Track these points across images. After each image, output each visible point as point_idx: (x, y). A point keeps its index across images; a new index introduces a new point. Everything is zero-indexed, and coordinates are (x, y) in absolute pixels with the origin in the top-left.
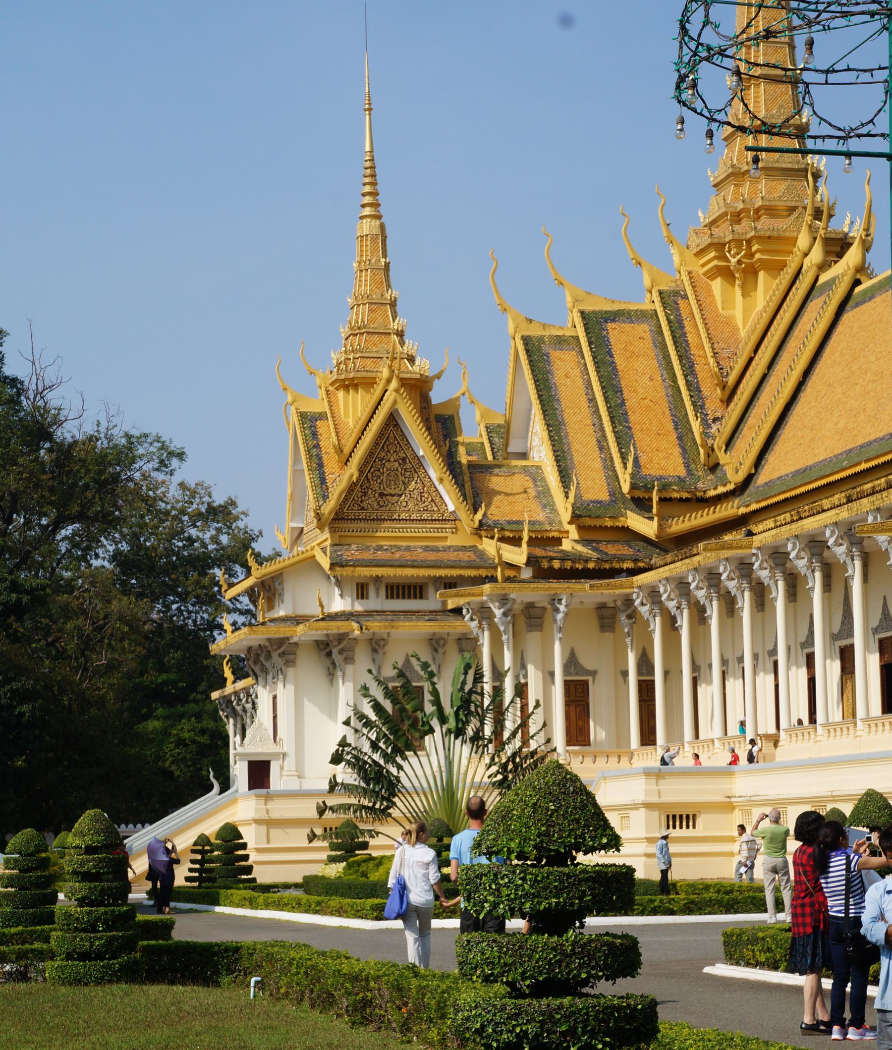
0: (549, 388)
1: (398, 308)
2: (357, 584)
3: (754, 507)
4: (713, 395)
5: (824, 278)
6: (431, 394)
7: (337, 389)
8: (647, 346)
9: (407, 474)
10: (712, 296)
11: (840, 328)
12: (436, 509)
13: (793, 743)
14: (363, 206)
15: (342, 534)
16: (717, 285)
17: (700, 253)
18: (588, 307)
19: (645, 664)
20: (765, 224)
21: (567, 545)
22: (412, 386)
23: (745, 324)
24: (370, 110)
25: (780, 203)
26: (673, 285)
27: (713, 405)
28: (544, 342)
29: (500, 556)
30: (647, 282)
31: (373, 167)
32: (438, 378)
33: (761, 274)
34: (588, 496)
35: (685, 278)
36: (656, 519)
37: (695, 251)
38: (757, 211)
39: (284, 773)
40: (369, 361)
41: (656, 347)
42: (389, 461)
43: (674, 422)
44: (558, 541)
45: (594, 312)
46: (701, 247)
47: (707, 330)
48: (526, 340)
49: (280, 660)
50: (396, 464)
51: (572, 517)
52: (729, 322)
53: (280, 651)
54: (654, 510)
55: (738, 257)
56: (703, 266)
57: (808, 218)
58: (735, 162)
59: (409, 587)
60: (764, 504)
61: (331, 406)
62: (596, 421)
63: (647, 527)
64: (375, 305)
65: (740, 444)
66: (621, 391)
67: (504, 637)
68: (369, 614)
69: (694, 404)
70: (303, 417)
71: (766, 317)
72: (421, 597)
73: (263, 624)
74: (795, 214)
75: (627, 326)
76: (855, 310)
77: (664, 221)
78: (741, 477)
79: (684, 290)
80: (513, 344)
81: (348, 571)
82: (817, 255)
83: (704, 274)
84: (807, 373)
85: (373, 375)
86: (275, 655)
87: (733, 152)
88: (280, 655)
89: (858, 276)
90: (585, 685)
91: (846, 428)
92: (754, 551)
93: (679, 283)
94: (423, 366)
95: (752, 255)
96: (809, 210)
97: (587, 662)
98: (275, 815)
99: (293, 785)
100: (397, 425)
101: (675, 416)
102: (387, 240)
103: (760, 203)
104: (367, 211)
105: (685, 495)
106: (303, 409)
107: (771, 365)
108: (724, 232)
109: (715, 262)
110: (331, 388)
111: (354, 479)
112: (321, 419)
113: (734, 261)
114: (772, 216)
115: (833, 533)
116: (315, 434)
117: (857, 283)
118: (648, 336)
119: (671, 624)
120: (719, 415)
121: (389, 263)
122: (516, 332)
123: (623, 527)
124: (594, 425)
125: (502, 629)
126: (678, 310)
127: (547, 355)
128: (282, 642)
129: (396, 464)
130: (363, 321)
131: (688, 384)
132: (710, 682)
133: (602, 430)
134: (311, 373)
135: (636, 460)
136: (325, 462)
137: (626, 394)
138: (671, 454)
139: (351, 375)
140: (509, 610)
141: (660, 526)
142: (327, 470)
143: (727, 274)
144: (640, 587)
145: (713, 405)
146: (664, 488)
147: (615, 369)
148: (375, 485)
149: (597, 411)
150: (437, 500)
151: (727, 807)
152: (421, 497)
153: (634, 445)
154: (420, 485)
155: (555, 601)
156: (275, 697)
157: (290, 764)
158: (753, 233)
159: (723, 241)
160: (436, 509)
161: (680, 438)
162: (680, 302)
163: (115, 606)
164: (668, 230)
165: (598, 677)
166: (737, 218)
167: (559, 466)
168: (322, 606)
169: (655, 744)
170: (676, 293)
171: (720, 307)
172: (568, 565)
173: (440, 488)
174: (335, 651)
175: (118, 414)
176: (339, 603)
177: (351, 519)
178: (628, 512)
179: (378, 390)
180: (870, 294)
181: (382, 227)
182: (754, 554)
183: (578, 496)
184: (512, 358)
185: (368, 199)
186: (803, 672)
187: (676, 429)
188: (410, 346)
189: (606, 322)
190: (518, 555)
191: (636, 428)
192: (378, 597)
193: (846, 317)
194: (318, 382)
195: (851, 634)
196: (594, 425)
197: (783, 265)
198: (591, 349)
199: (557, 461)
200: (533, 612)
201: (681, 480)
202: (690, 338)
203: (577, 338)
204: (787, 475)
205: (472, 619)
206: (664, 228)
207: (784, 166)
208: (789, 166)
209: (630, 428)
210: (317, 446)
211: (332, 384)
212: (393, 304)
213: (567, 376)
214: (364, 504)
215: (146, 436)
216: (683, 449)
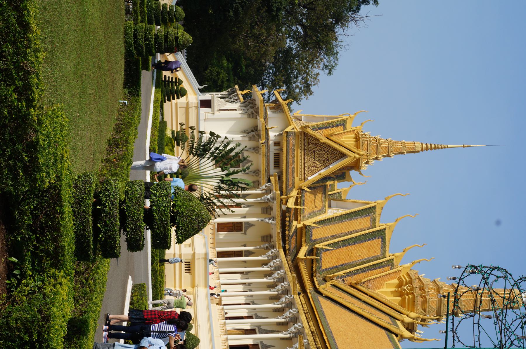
0: (356, 216)
1: (387, 158)
2: (280, 142)
3: (310, 296)
4: (353, 280)
5: (399, 323)
6: (353, 171)
7: (355, 134)
8: (372, 254)
9: (322, 161)
10: (392, 279)
11: (379, 329)
13: (222, 342)
14: (426, 144)
15: (299, 136)
16: (396, 281)
17: (408, 275)
18: (387, 231)
19: (249, 253)
20: (420, 300)
21: (295, 223)
22: (357, 163)
23: (381, 292)
24: (464, 147)
25: (427, 306)
27: (349, 280)
28: (373, 214)
29: (290, 197)
30: (397, 254)
31: (441, 148)
32: (360, 173)
33: (400, 298)
34: (314, 231)
35: (399, 269)
36: (305, 258)
37: (409, 273)
38: (425, 297)
39: (206, 114)
40: (366, 146)
41: (372, 258)
43: (343, 265)
44: (296, 220)
45: (385, 234)
46: (410, 275)
47: (378, 278)
48: (374, 207)
49: (250, 112)
50: (326, 157)
52: (381, 286)
53: (254, 112)
54: (308, 257)
55: (407, 289)
56: (403, 276)
57: (422, 316)
58: (444, 288)
59: (279, 162)
60: (311, 299)
61: (349, 132)
62: (343, 235)
63: (302, 254)
64: (388, 149)
65: (334, 290)
66: (355, 244)
67: (259, 199)
68: (268, 146)
69: (350, 272)
70: (345, 121)
71: (383, 300)
72: (275, 167)
73: (264, 105)
74: (423, 312)
75: (380, 246)
76: (386, 335)
77: (421, 261)
78: (321, 290)
79: (394, 269)
80: (373, 202)
81: (285, 138)
82: (407, 320)
83: (400, 276)
84: (362, 316)
85: (361, 148)
86: (252, 110)
87: (447, 287)
88: (252, 112)
89: (399, 336)
90: (241, 230)
92: (293, 296)
93: (397, 266)
94: (364, 167)
95: (407, 295)
96: (425, 317)
97: (250, 231)
98: (190, 110)
99: (202, 117)
100: (341, 157)
102: (413, 154)
103: (427, 298)
104: (424, 146)
105: (314, 269)
106: (348, 121)
107: (364, 302)
108: (416, 284)
109: (404, 281)
110: (356, 132)
111: (321, 141)
112: (344, 128)
113: (405, 288)
114: (422, 303)
115: (300, 326)
116: (338, 125)
117: (397, 335)
118: (376, 254)
119: (264, 263)
120: (345, 282)
123: (302, 245)
125: (262, 198)
126: (386, 266)
127: (369, 215)
128: (257, 113)
129: (326, 157)
130: (382, 144)
131: (357, 270)
132: (242, 278)
133: (340, 237)
134: (362, 124)
135: (328, 250)
136: (327, 130)
137: (353, 246)
139: (361, 140)
140: (270, 201)
141: (302, 259)
142: (324, 130)
143: (400, 285)
144: (278, 251)
145: (349, 280)
146: (317, 261)
147: (364, 242)
148: (318, 149)
149: (347, 235)
150: (312, 173)
151: (193, 285)
154: (318, 166)
155: (273, 218)
156: (236, 110)
157: (210, 116)
158: (416, 295)
159: (413, 283)
161: (336, 267)
162: (389, 267)
163: (271, 48)
164: (417, 262)
165: (244, 235)
166: (422, 289)
167: (325, 220)
168: (271, 128)
169: (218, 257)
170: (393, 265)
172: (287, 224)
173: (317, 174)
174: (254, 133)
175: (346, 49)
176: (272, 135)
178: (307, 247)
180: (392, 341)
181: (418, 152)
182: (291, 296)
183: (314, 227)
184: (367, 202)
185: (429, 146)
186: (246, 315)
187: (340, 265)
188: (372, 162)
189: (382, 238)
190: (291, 204)
192: (276, 150)
193: (383, 332)
194: (358, 127)
195: (260, 333)
197: (403, 307)
198: (371, 232)
199: (327, 219)
200: (269, 210)
201: (320, 267)
202: (375, 271)
203: (375, 227)
204: (322, 308)
205: (266, 186)
206: (418, 261)
207: (442, 307)
208: (442, 309)
209: (340, 247)
210: (333, 126)
211: (357, 132)
212: (388, 156)
214: (311, 145)
215: (337, 60)
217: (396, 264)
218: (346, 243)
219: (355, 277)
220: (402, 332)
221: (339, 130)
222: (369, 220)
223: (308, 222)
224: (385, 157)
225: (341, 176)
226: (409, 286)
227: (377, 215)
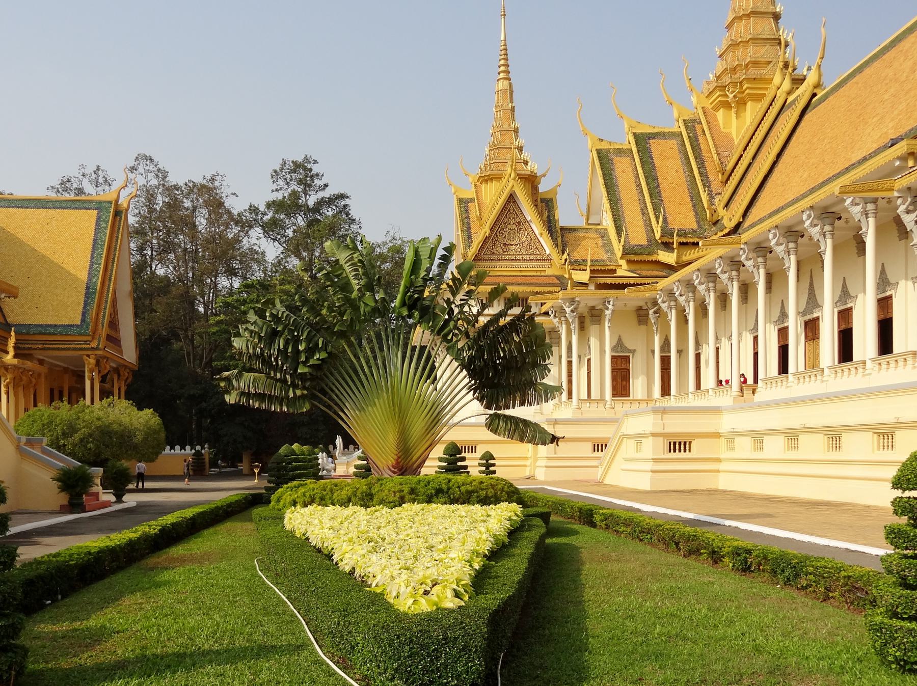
0: (611, 179)
4: (716, 178)
9: (521, 232)
10: (716, 120)
11: (802, 124)
12: (538, 253)
16: (720, 114)
18: (638, 131)
19: (666, 345)
20: (752, 72)
21: (620, 272)
22: (526, 179)
23: (737, 136)
24: (505, 15)
25: (762, 60)
28: (610, 153)
30: (676, 115)
31: (506, 50)
32: (544, 176)
33: (749, 104)
34: (633, 243)
35: (700, 112)
37: (706, 95)
38: (747, 65)
41: (680, 153)
42: (510, 224)
43: (690, 196)
44: (615, 271)
45: (642, 134)
46: (711, 90)
47: (713, 140)
48: (599, 152)
51: (623, 254)
52: (728, 137)
55: (734, 94)
56: (711, 104)
58: (733, 38)
61: (477, 195)
65: (733, 206)
75: (662, 141)
77: (687, 77)
78: (733, 224)
82: (787, 85)
84: (779, 155)
85: (500, 172)
91: (809, 177)
101: (691, 193)
107: (754, 157)
108: (727, 80)
111: (487, 234)
112: (471, 202)
113: (731, 96)
116: (467, 211)
117: (814, 95)
119: (683, 319)
120: (720, 191)
121: (514, 107)
122: (592, 147)
123: (656, 261)
124: (639, 200)
131: (700, 173)
134: (466, 175)
135: (665, 219)
136: (472, 227)
140: (576, 309)
141: (678, 257)
142: (473, 231)
143: (726, 105)
144: (661, 290)
145: (716, 186)
152: (530, 246)
153: (664, 208)
154: (529, 239)
155: (605, 301)
158: (744, 77)
159: (724, 84)
160: (538, 253)
161: (694, 206)
164: (690, 84)
165: (636, 354)
166: (734, 70)
167: (616, 224)
169: (670, 395)
170: (694, 121)
171: (722, 127)
179: (504, 181)
180: (826, 97)
187: (692, 201)
189: (649, 139)
191: (666, 201)
196: (639, 200)
198: (639, 154)
199: (615, 221)
202: (702, 146)
206: (687, 81)
207: (764, 37)
208: (768, 37)
209: (662, 201)
210: (468, 217)
211: (478, 181)
213: (623, 172)
214: (494, 251)
216: (696, 213)
217: (693, 116)
218: (655, 192)
219: (711, 178)
220: (809, 86)
222: (618, 159)
223: (618, 249)
224: (518, 136)
225: (547, 205)
226: (728, 91)
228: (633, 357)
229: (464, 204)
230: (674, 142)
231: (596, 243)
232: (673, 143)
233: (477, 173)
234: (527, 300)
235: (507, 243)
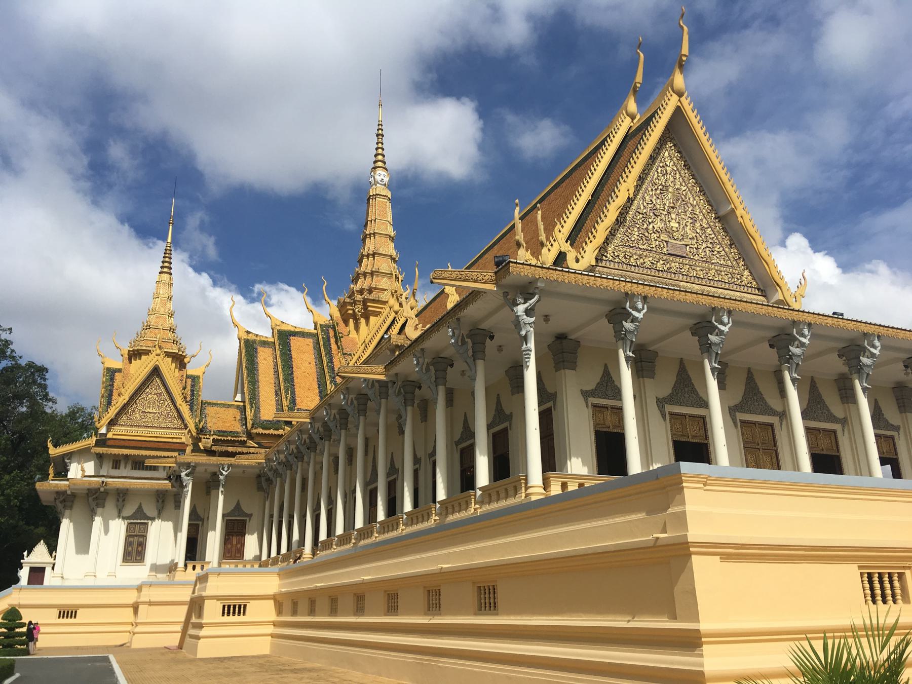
2: (114, 460)
9: (162, 402)
15: (114, 433)
26: (328, 322)
28: (256, 343)
40: (150, 342)
43: (318, 384)
62: (277, 382)
75: (301, 339)
85: (148, 349)
99: (57, 582)
111: (125, 401)
113: (357, 310)
118: (311, 345)
124: (275, 383)
126: (329, 333)
127: (256, 349)
138: (314, 399)
152: (168, 415)
177: (122, 425)
179: (151, 356)
187: (319, 387)
192: (125, 467)
196: (275, 383)
207: (384, 271)
208: (387, 272)
209: (294, 385)
210: (112, 385)
213: (265, 359)
214: (132, 417)
221: (118, 376)
227: (258, 339)
228: (249, 522)
229: (111, 373)
230: (311, 340)
231: (235, 417)
232: (310, 341)
233: (126, 348)
234: (144, 463)
235: (146, 411)
